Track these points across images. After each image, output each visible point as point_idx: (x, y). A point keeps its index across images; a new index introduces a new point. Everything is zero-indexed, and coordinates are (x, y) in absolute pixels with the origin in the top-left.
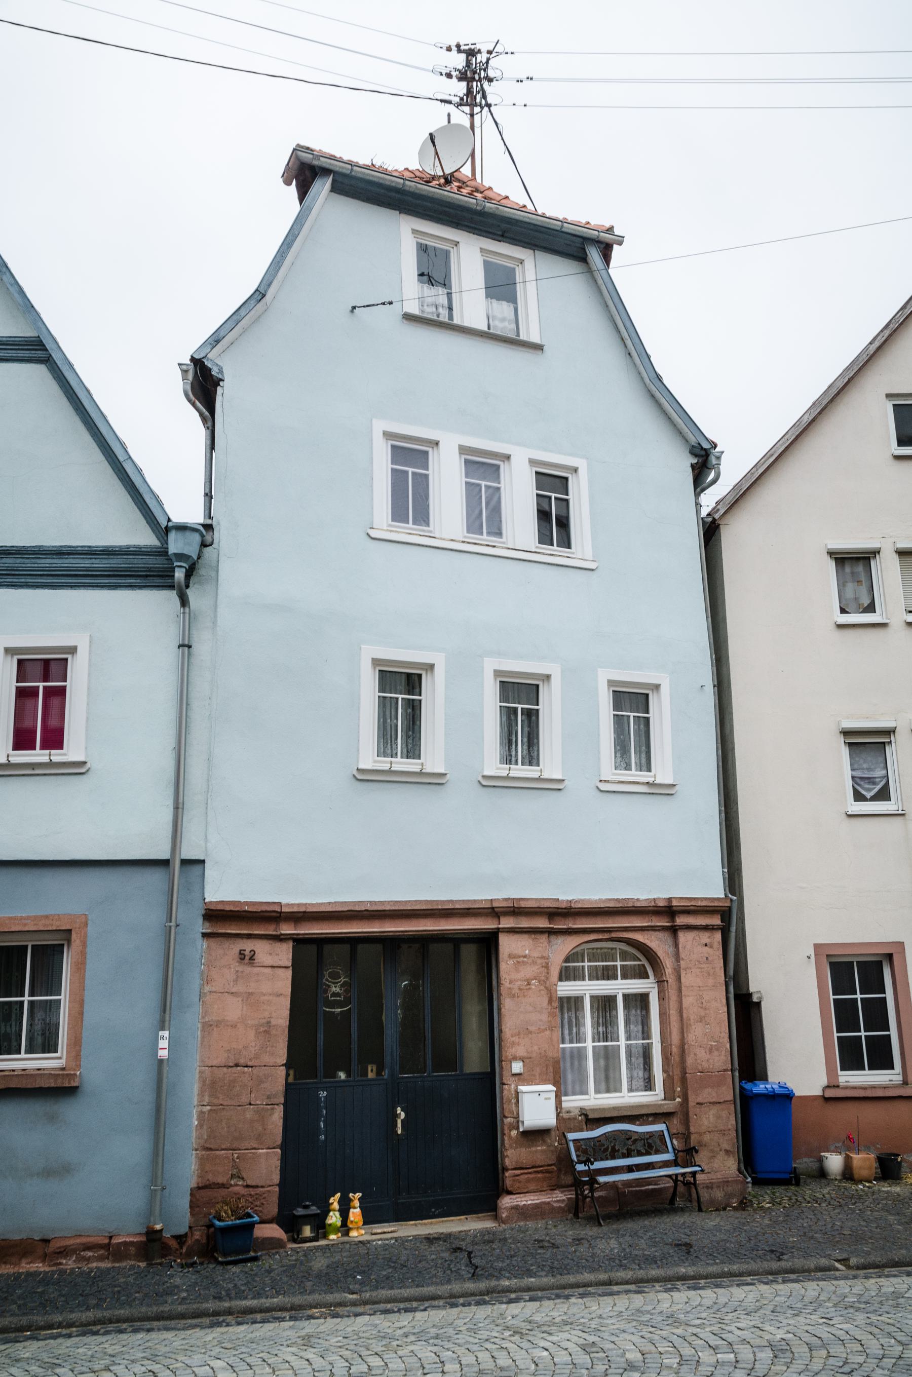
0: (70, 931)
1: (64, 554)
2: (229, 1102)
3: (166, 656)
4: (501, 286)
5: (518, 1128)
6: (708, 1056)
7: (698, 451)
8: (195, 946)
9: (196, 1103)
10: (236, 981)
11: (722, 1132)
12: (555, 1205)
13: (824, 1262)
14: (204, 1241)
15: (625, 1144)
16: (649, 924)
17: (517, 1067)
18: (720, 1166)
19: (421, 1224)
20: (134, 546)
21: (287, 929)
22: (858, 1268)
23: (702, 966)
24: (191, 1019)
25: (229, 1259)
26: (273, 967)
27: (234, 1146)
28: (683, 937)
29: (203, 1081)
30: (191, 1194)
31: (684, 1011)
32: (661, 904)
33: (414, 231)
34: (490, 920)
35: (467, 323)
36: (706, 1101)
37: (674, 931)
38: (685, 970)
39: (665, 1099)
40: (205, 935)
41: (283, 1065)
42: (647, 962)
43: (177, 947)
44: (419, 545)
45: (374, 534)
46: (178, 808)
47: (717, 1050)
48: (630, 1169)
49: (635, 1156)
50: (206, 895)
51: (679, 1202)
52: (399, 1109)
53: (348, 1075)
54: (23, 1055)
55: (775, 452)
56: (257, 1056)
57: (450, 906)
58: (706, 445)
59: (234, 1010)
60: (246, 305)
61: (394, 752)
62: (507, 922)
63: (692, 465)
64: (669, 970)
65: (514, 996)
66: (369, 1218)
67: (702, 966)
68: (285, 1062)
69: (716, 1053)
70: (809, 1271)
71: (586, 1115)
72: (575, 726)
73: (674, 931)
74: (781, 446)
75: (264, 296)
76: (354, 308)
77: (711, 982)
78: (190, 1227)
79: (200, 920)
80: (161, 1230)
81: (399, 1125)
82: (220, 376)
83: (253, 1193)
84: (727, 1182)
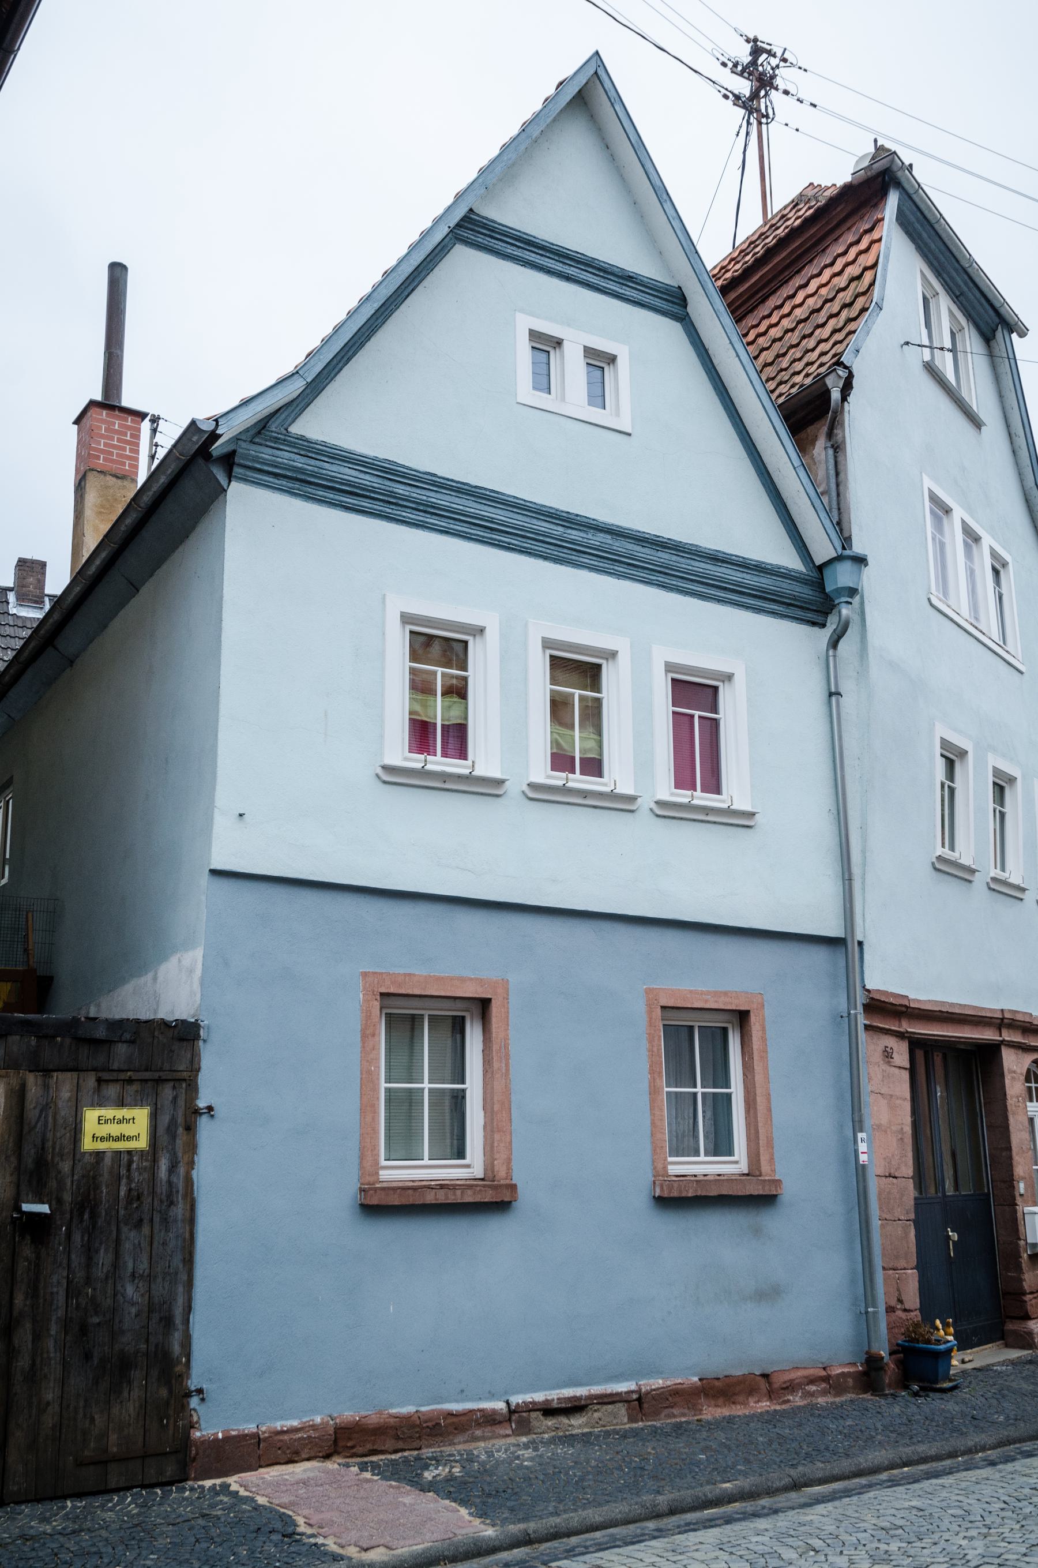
1: (718, 560)
20: (786, 569)
50: (866, 982)
54: (702, 1158)
62: (1007, 1036)
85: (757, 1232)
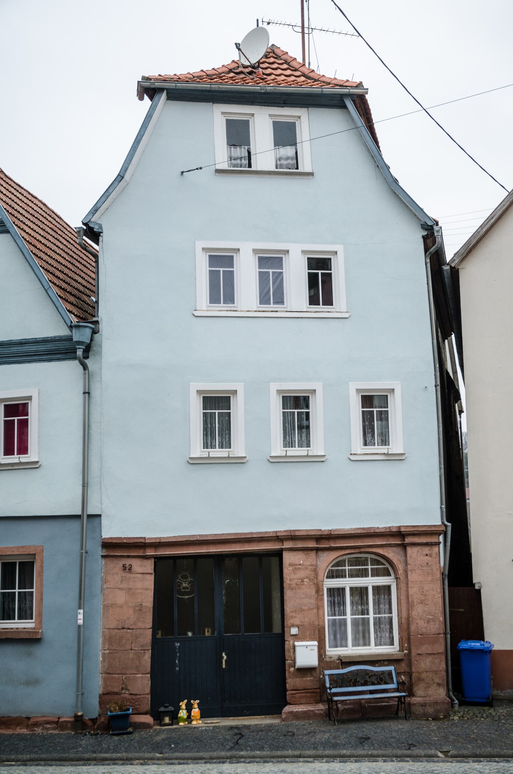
0: (35, 554)
1: (23, 344)
2: (119, 648)
3: (79, 399)
4: (285, 135)
5: (294, 666)
6: (426, 625)
7: (426, 227)
8: (97, 563)
9: (101, 649)
10: (122, 581)
11: (435, 672)
12: (317, 712)
13: (433, 752)
14: (106, 722)
15: (364, 678)
16: (387, 543)
17: (294, 631)
18: (433, 691)
19: (237, 719)
21: (150, 552)
22: (452, 757)
23: (424, 568)
24: (98, 603)
25: (116, 732)
26: (143, 573)
27: (123, 673)
28: (409, 550)
29: (104, 636)
30: (100, 697)
31: (410, 597)
32: (394, 530)
33: (223, 113)
34: (277, 543)
35: (259, 169)
36: (424, 653)
37: (404, 546)
38: (411, 571)
39: (399, 651)
40: (103, 557)
41: (150, 628)
42: (384, 567)
43: (87, 563)
44: (227, 317)
45: (197, 313)
46: (85, 485)
47: (433, 621)
48: (372, 692)
49: (370, 685)
50: (103, 535)
51: (401, 714)
52: (224, 653)
53: (193, 634)
55: (495, 215)
56: (135, 623)
57: (250, 536)
58: (430, 223)
59: (121, 598)
60: (113, 185)
61: (213, 444)
62: (287, 545)
63: (423, 237)
64: (401, 572)
65: (292, 589)
66: (203, 715)
67: (424, 568)
68: (151, 626)
69: (432, 623)
70: (420, 756)
71: (341, 660)
72: (335, 421)
73: (404, 546)
74: (499, 210)
75: (123, 178)
76: (182, 172)
77: (430, 578)
78: (100, 715)
79: (100, 548)
80: (82, 716)
81: (224, 663)
82: (100, 230)
83: (134, 698)
84: (436, 703)
85: (29, 655)
